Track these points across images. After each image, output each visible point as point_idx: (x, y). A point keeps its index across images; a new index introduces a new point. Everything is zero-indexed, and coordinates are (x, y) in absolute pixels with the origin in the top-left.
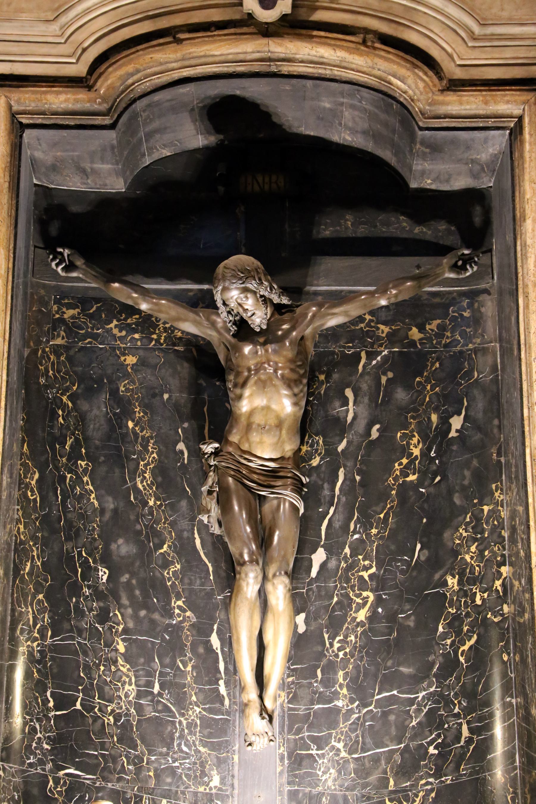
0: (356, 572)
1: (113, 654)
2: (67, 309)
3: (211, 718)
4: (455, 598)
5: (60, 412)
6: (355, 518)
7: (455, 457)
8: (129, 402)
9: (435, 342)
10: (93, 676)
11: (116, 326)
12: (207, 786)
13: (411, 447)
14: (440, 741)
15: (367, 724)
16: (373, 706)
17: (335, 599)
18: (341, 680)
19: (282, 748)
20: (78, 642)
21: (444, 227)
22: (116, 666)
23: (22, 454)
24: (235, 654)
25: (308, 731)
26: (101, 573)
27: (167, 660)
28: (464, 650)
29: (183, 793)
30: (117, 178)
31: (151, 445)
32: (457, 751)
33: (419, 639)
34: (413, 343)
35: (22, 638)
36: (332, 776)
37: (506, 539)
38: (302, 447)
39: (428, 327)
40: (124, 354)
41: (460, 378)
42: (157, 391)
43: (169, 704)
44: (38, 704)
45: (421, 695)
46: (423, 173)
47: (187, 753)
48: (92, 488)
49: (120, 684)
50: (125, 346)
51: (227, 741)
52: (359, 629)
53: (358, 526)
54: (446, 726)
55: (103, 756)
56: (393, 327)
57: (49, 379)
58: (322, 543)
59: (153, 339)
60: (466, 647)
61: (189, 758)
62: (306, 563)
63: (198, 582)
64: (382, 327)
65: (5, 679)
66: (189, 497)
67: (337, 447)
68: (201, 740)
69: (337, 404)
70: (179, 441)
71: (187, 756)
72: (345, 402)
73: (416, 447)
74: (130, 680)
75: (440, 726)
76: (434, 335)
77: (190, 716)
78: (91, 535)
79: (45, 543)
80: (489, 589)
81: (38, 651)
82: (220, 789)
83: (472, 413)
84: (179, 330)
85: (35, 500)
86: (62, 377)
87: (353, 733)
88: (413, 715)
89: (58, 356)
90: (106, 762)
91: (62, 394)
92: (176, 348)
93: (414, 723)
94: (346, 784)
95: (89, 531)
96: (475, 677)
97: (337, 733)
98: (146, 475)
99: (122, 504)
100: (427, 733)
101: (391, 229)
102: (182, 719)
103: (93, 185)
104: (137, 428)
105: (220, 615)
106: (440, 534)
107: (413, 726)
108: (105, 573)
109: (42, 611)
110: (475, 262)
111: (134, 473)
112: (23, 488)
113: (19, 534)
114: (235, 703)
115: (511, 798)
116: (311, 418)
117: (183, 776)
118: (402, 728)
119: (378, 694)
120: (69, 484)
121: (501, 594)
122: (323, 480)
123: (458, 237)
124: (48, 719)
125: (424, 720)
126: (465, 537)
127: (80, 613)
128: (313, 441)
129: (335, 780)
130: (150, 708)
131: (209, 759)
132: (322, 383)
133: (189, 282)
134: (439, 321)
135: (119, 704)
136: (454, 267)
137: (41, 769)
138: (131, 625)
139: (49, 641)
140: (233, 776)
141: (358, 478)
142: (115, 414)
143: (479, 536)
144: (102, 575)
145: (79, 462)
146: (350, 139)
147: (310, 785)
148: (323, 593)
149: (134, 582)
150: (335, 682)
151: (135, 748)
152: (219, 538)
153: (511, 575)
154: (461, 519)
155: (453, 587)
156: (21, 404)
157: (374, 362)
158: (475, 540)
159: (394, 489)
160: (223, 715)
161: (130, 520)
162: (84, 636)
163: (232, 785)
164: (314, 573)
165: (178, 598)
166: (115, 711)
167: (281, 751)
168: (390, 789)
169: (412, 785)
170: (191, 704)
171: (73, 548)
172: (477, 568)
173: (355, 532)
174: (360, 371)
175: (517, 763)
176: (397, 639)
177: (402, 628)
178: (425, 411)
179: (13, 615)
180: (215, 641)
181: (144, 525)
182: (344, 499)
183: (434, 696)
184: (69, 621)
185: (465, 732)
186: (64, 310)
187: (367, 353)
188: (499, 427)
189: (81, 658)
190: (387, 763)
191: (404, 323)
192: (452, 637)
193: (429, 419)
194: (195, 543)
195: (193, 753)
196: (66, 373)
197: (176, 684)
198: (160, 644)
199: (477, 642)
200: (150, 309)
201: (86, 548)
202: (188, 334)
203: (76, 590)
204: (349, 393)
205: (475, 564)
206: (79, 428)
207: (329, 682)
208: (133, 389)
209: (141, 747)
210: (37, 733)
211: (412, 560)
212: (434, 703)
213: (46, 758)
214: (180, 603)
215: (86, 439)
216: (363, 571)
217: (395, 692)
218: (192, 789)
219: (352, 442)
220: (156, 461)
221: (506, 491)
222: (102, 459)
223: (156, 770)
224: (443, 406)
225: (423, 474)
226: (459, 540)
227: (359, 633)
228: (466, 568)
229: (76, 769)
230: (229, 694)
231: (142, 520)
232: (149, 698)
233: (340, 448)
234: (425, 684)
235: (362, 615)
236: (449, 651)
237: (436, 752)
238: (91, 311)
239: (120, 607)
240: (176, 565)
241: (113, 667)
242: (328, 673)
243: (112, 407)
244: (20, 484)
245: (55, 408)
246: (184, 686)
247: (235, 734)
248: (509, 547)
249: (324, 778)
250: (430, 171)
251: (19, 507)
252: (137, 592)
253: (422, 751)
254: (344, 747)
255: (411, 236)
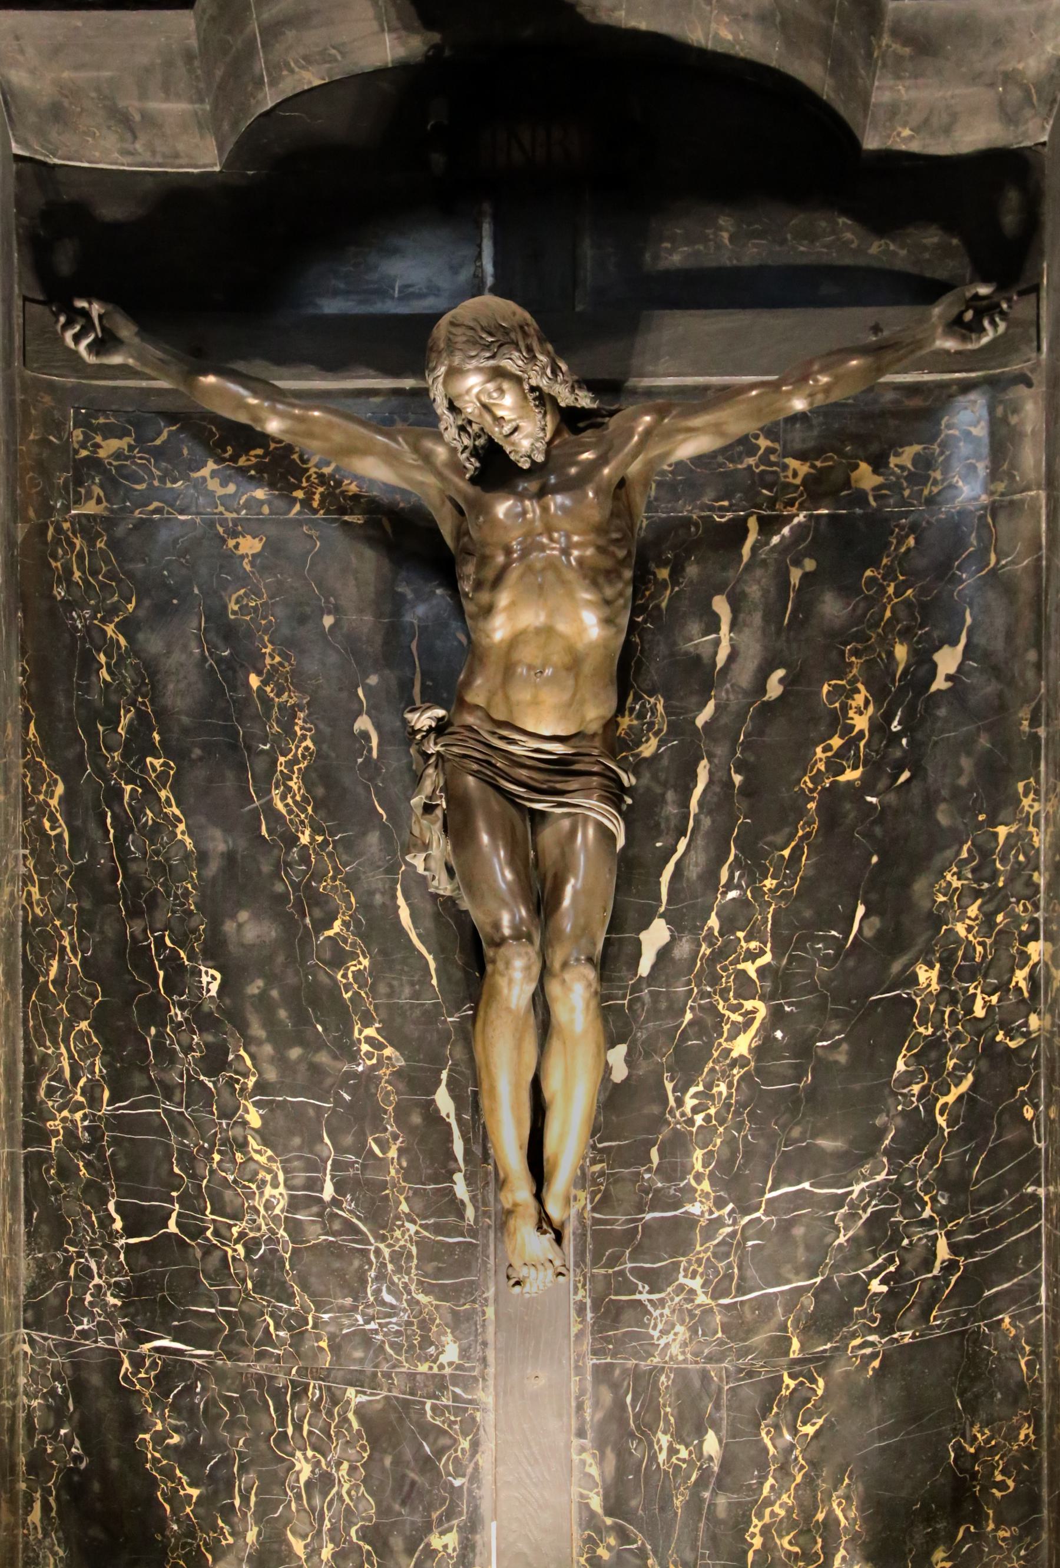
0: (731, 964)
1: (238, 1131)
2: (105, 438)
3: (438, 1242)
4: (932, 1007)
5: (102, 658)
6: (732, 858)
7: (942, 731)
8: (250, 635)
9: (907, 493)
10: (199, 1171)
11: (214, 474)
12: (435, 1361)
13: (851, 713)
14: (892, 1269)
15: (750, 1243)
16: (762, 1211)
17: (689, 1016)
18: (698, 1166)
19: (581, 1292)
20: (164, 1110)
21: (935, 240)
22: (245, 1153)
23: (26, 744)
24: (488, 1125)
25: (632, 1259)
26: (205, 979)
27: (348, 1140)
28: (946, 1104)
29: (388, 1376)
30: (202, 137)
31: (300, 722)
32: (925, 1287)
33: (857, 1086)
34: (860, 497)
35: (50, 1103)
36: (680, 1338)
37: (1042, 888)
38: (619, 719)
39: (893, 461)
40: (235, 534)
41: (959, 568)
42: (308, 610)
43: (355, 1220)
44: (92, 1225)
45: (857, 1189)
46: (893, 111)
47: (392, 1307)
48: (177, 812)
49: (254, 1186)
50: (235, 515)
51: (473, 1282)
52: (735, 1071)
53: (737, 874)
54: (906, 1242)
55: (226, 1315)
56: (818, 464)
57: (74, 589)
58: (662, 909)
59: (295, 500)
60: (950, 1099)
61: (395, 1315)
62: (629, 949)
63: (407, 991)
64: (793, 463)
65: (22, 1179)
66: (384, 827)
67: (695, 718)
68: (420, 1283)
69: (694, 627)
70: (359, 713)
71: (393, 1312)
72: (713, 625)
73: (861, 713)
74: (276, 1176)
75: (894, 1242)
76: (906, 478)
77: (398, 1240)
78: (182, 904)
79: (86, 923)
80: (1003, 987)
81: (85, 1128)
82: (459, 1367)
83: (981, 640)
84: (356, 477)
85: (60, 836)
86: (103, 586)
87: (720, 1260)
88: (841, 1224)
89: (91, 539)
90: (233, 1325)
91: (103, 620)
92: (346, 518)
93: (842, 1239)
94: (706, 1351)
95: (176, 897)
96: (965, 1152)
97: (689, 1262)
98: (291, 784)
99: (242, 844)
100: (868, 1256)
101: (819, 247)
102: (382, 1246)
103: (147, 157)
104: (268, 689)
105: (454, 1052)
106: (906, 884)
107: (840, 1245)
108: (214, 978)
109: (88, 1053)
110: (1003, 315)
111: (266, 780)
112: (33, 813)
113: (31, 904)
114: (486, 1214)
115: (1027, 1364)
116: (639, 659)
117: (387, 1346)
118: (819, 1248)
119: (771, 1190)
120: (130, 805)
121: (1026, 995)
122: (665, 785)
123: (966, 260)
124: (115, 1253)
125: (862, 1233)
126: (957, 889)
127: (165, 1055)
128: (643, 706)
129: (684, 1344)
130: (318, 1228)
131: (436, 1315)
132: (663, 585)
133: (372, 372)
134: (917, 448)
135: (254, 1221)
136: (957, 326)
137: (105, 1340)
138: (272, 1075)
139: (106, 1109)
140: (485, 1344)
141: (737, 779)
142: (220, 661)
143: (986, 885)
144: (208, 983)
145: (149, 760)
146: (730, 37)
147: (635, 1355)
148: (663, 1005)
149: (275, 993)
150: (686, 1170)
151: (289, 1298)
152: (450, 903)
153: (1047, 958)
154: (949, 853)
155: (929, 985)
156: (15, 641)
157: (775, 540)
158: (978, 894)
159: (813, 799)
160: (463, 1235)
161: (259, 872)
162: (177, 1099)
163: (484, 1360)
164: (645, 967)
165: (367, 1022)
166: (246, 1234)
167: (579, 1297)
168: (792, 1356)
169: (834, 1349)
170: (398, 1218)
171: (144, 931)
172: (979, 949)
173: (729, 886)
174: (746, 558)
175: (1043, 1302)
176: (812, 1090)
177: (823, 1067)
178: (882, 639)
179: (28, 1062)
180: (444, 1101)
181: (292, 882)
182: (707, 822)
183: (884, 1190)
184: (145, 1070)
185: (943, 1251)
186: (98, 439)
187: (762, 521)
188: (1038, 666)
189: (173, 1140)
190: (787, 1312)
191: (840, 453)
192: (923, 1079)
193: (891, 654)
194: (398, 917)
195: (405, 1305)
196: (111, 575)
197: (368, 1182)
198: (334, 1110)
199: (973, 1087)
200: (285, 432)
201: (171, 931)
202: (372, 482)
203: (156, 1012)
204: (721, 606)
205: (975, 941)
206: (144, 689)
207: (675, 1171)
208: (256, 608)
209: (301, 1297)
210: (93, 1278)
211: (846, 938)
212: (883, 1201)
213: (115, 1322)
214: (370, 1032)
215: (162, 713)
216: (745, 960)
217: (806, 1185)
218: (406, 1367)
219: (726, 706)
220: (311, 755)
221: (1047, 793)
222: (197, 752)
223: (332, 1338)
224: (921, 627)
225: (874, 768)
226: (945, 895)
227: (736, 1078)
228: (956, 950)
229: (174, 1340)
230: (473, 1199)
231: (287, 873)
232: (315, 1209)
233: (701, 720)
234: (866, 1169)
235: (742, 1045)
236: (917, 1107)
237: (884, 1289)
238: (158, 442)
239: (248, 1042)
240: (361, 958)
241: (238, 1155)
242: (673, 1155)
243: (213, 647)
244: (25, 806)
245: (90, 650)
246: (384, 1185)
247: (486, 1270)
248: (1048, 903)
249: (662, 1342)
250: (911, 105)
251: (27, 852)
252: (283, 1014)
253: (857, 1289)
254: (703, 1286)
255: (861, 262)
